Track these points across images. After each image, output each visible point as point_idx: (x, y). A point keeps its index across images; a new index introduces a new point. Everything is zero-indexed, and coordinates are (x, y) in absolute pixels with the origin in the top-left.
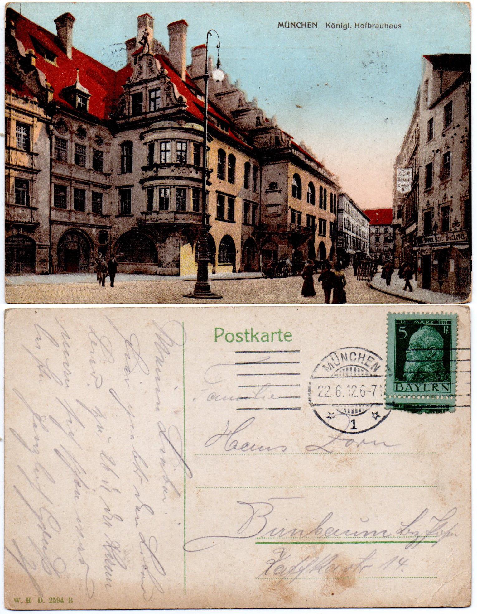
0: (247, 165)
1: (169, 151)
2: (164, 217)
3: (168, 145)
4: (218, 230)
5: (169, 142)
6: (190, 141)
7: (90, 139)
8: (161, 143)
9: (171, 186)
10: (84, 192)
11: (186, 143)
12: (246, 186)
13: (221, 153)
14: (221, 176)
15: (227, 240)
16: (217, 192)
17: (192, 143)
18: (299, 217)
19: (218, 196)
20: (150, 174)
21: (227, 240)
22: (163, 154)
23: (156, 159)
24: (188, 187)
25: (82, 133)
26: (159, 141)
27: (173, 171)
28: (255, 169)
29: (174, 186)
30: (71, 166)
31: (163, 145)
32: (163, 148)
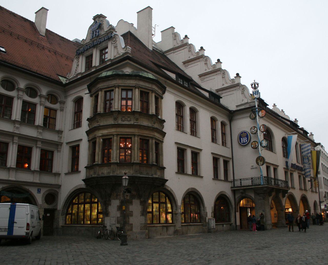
0: (213, 120)
1: (112, 100)
2: (105, 171)
3: (113, 93)
4: (178, 185)
5: (113, 90)
6: (135, 87)
7: (41, 96)
8: (106, 92)
9: (114, 135)
10: (30, 149)
11: (132, 90)
12: (214, 140)
13: (179, 106)
14: (180, 127)
15: (193, 197)
16: (176, 143)
17: (137, 90)
18: (275, 170)
19: (179, 149)
20: (96, 125)
21: (193, 197)
22: (108, 102)
23: (100, 109)
24: (135, 135)
25: (32, 92)
26: (103, 91)
27: (115, 119)
28: (223, 124)
29: (117, 135)
30: (15, 122)
31: (108, 94)
32: (108, 98)
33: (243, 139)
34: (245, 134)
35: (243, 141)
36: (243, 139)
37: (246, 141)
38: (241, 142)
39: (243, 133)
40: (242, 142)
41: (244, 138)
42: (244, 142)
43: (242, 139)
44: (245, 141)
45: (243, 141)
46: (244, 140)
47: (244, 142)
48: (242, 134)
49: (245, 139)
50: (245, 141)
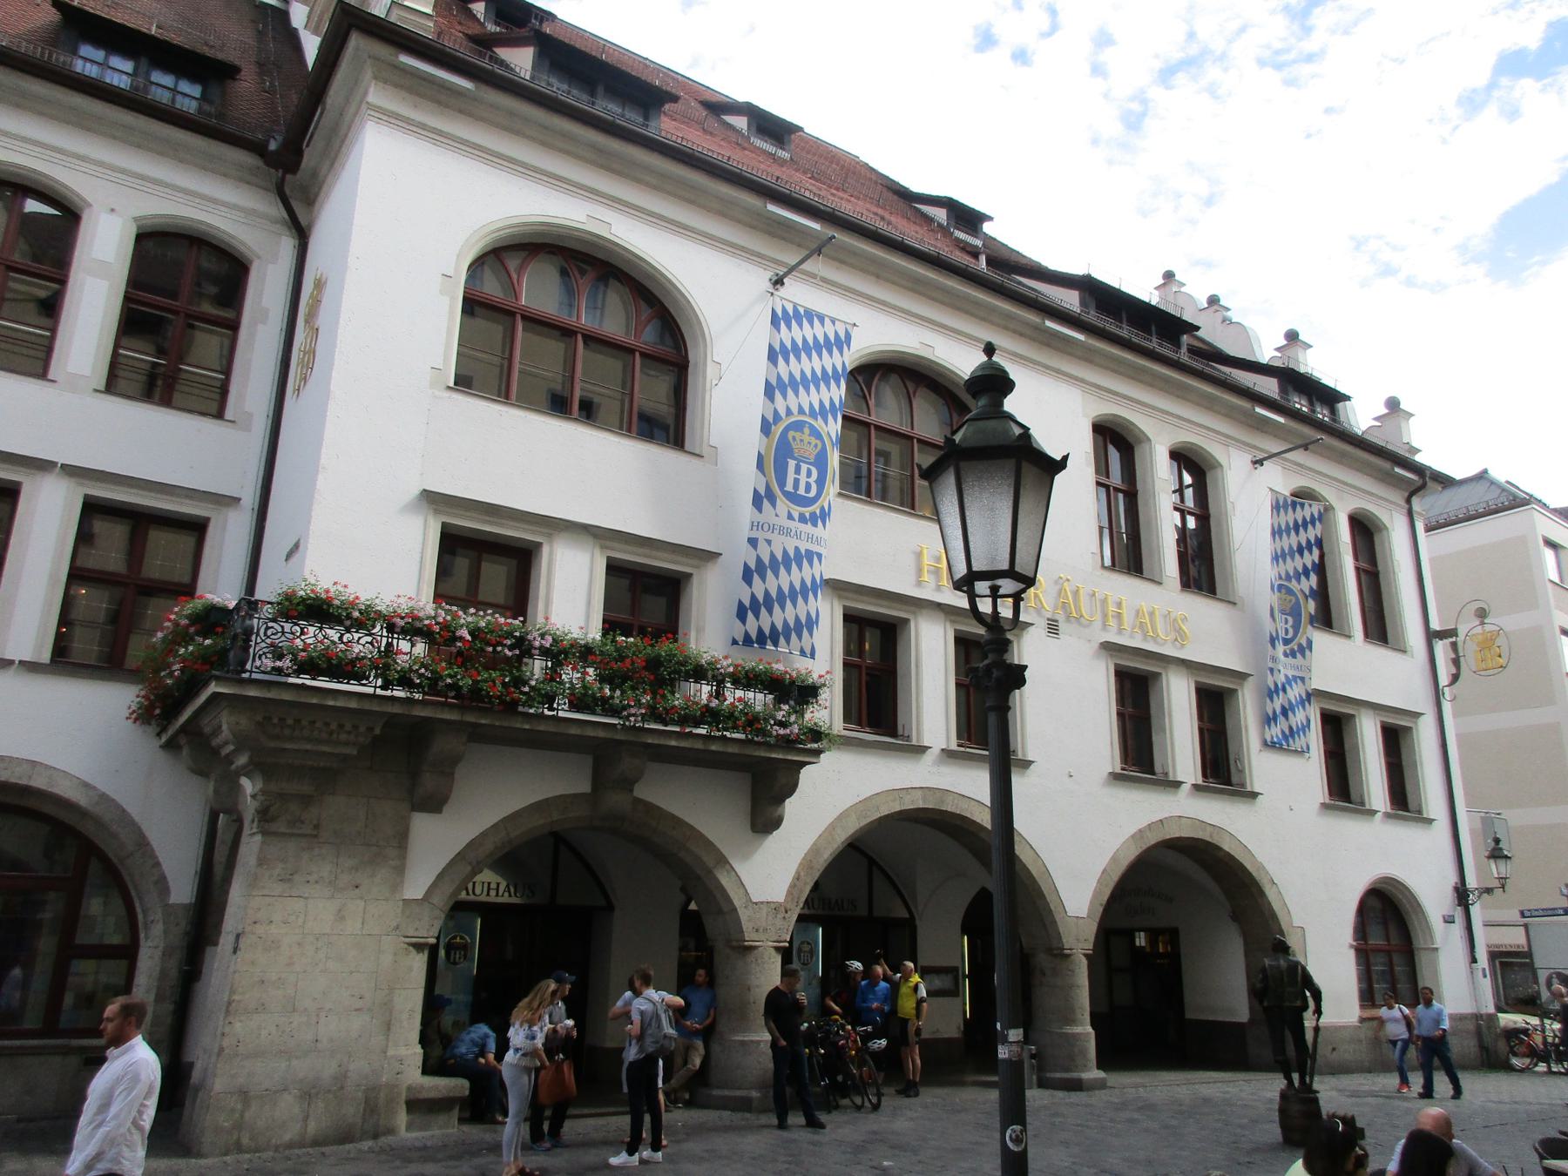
33: (798, 470)
34: (814, 441)
35: (796, 482)
36: (798, 470)
37: (813, 493)
38: (782, 484)
39: (807, 431)
40: (789, 487)
41: (804, 467)
42: (801, 491)
43: (792, 464)
44: (808, 488)
45: (796, 482)
46: (803, 478)
47: (801, 491)
48: (797, 435)
49: (809, 474)
50: (808, 488)
